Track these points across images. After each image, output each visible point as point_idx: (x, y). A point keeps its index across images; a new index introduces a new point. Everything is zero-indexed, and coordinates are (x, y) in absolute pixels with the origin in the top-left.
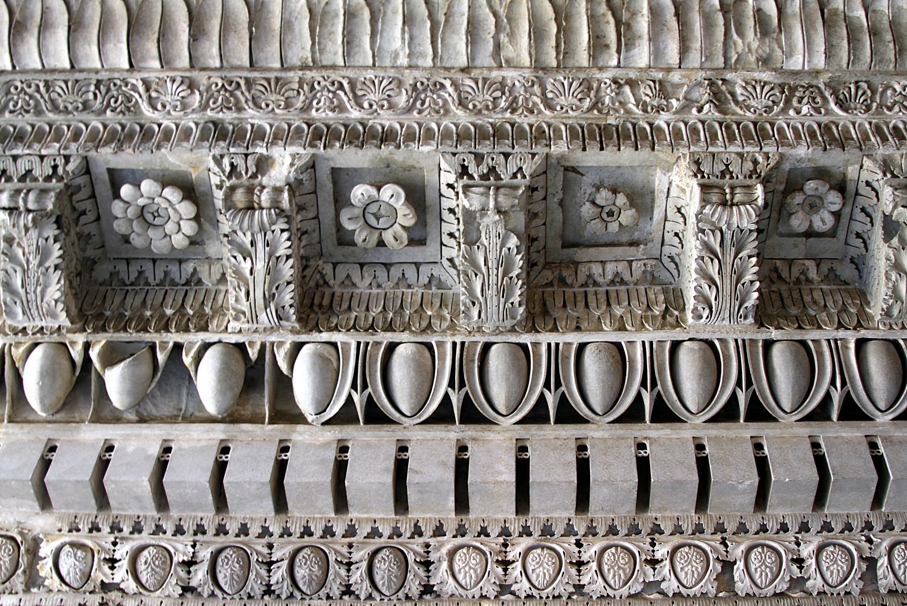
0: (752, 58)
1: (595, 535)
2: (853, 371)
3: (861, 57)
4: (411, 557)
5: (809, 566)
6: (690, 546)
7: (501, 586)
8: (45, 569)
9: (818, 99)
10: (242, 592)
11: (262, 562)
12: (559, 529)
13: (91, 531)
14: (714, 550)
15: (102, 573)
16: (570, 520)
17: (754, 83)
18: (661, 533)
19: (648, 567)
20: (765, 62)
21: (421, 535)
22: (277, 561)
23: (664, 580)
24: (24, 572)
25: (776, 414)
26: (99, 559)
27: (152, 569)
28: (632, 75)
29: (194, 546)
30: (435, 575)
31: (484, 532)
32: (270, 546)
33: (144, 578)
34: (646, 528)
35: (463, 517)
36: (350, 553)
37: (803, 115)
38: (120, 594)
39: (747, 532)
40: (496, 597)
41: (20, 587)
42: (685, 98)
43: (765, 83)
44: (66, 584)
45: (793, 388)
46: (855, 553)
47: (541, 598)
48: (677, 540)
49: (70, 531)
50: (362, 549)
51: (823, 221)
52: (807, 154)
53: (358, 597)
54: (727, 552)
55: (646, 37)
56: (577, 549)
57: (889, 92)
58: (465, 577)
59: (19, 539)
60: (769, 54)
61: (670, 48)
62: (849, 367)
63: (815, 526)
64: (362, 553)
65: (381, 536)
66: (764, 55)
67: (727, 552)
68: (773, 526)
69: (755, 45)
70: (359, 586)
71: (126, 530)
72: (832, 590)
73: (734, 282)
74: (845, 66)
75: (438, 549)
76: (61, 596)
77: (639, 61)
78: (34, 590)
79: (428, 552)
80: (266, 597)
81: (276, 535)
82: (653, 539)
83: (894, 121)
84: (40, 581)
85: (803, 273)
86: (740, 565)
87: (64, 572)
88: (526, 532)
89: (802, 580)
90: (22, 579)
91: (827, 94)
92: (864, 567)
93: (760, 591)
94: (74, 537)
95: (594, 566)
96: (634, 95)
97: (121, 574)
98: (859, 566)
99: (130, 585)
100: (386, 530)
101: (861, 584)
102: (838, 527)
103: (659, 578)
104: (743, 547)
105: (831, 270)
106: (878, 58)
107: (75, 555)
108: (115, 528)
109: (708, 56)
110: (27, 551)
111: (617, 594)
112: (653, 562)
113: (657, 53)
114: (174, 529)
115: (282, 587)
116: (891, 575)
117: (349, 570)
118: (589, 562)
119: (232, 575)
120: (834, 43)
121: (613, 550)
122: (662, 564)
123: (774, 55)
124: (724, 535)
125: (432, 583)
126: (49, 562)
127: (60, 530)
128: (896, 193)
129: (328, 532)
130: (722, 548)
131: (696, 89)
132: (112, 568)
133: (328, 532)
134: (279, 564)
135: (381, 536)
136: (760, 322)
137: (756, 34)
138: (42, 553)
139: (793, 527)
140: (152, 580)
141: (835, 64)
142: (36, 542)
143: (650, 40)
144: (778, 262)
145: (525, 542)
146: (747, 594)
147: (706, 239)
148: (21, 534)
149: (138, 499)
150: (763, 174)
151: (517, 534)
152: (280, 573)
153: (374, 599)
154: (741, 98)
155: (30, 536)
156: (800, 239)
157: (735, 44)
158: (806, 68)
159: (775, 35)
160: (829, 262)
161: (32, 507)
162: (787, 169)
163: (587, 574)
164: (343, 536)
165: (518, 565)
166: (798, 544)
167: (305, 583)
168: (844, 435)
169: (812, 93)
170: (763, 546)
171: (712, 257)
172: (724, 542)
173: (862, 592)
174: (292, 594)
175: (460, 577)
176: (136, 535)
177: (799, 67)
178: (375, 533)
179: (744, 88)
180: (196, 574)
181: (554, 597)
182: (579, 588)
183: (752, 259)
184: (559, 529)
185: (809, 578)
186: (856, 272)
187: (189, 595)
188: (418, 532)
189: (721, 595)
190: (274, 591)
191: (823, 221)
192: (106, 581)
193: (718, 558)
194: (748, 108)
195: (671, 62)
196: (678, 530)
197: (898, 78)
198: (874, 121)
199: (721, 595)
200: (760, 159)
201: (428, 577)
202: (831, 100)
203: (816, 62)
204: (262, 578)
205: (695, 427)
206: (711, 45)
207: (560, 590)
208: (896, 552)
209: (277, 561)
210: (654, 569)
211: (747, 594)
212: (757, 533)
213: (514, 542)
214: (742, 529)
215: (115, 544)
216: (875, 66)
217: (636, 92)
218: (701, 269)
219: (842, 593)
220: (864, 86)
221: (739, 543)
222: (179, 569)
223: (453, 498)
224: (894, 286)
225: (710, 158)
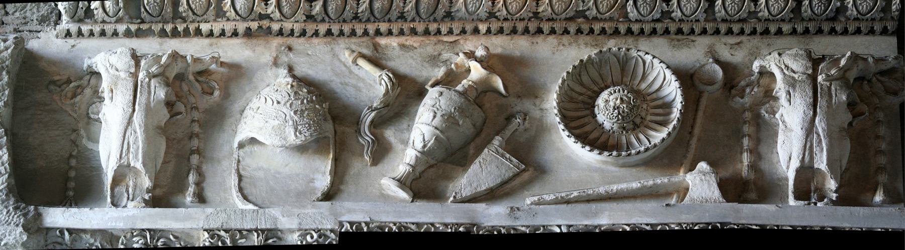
5: (673, 4)
7: (489, 13)
53: (406, 20)
76: (234, 23)
87: (238, 8)
90: (213, 13)
101: (705, 15)
116: (723, 11)
173: (706, 20)
207: (525, 16)
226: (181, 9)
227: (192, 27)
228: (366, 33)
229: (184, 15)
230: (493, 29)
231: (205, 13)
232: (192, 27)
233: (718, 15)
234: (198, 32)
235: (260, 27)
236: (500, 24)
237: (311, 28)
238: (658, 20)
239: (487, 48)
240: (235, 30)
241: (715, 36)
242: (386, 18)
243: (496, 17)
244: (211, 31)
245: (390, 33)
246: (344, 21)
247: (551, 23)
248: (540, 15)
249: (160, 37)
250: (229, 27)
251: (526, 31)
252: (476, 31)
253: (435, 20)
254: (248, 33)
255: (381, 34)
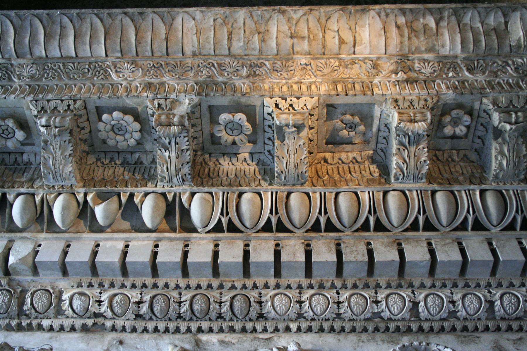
1: (346, 288)
4: (252, 299)
5: (458, 305)
6: (395, 294)
7: (298, 314)
8: (65, 305)
10: (166, 317)
11: (176, 302)
12: (328, 285)
13: (88, 287)
14: (408, 296)
15: (94, 308)
16: (333, 281)
18: (381, 287)
19: (374, 305)
20: (430, 50)
21: (257, 288)
22: (184, 302)
23: (382, 311)
24: (54, 307)
26: (93, 301)
27: (120, 306)
29: (141, 294)
30: (265, 308)
31: (289, 287)
32: (180, 294)
33: (116, 310)
34: (372, 284)
35: (279, 279)
36: (221, 297)
38: (103, 318)
39: (425, 287)
40: (296, 319)
41: (52, 315)
44: (76, 314)
46: (482, 298)
47: (319, 320)
48: (388, 291)
49: (78, 287)
50: (227, 295)
53: (225, 320)
54: (415, 297)
56: (337, 296)
58: (280, 309)
59: (52, 291)
63: (461, 284)
64: (227, 297)
65: (236, 288)
67: (415, 297)
68: (438, 284)
70: (226, 314)
71: (106, 286)
72: (471, 317)
73: (416, 161)
74: (471, 52)
75: (266, 295)
76: (73, 320)
78: (60, 317)
79: (261, 297)
80: (178, 320)
81: (183, 288)
82: (376, 291)
84: (62, 312)
85: (450, 157)
86: (422, 304)
87: (75, 307)
88: (311, 287)
89: (455, 312)
90: (53, 311)
91: (462, 66)
92: (488, 305)
93: (433, 318)
94: (80, 290)
95: (346, 304)
97: (104, 308)
98: (485, 305)
99: (109, 314)
100: (239, 285)
102: (473, 286)
103: (380, 310)
104: (423, 295)
105: (465, 155)
107: (81, 299)
108: (101, 285)
110: (56, 297)
111: (359, 318)
112: (377, 302)
114: (131, 285)
115: (187, 314)
116: (502, 310)
117: (220, 306)
118: (343, 302)
119: (161, 308)
121: (356, 296)
122: (381, 303)
124: (413, 289)
125: (263, 312)
126: (67, 302)
127: (73, 287)
129: (210, 287)
130: (412, 295)
132: (100, 305)
133: (210, 287)
134: (185, 303)
135: (236, 288)
138: (64, 298)
139: (449, 284)
140: (120, 311)
142: (61, 293)
145: (312, 292)
146: (426, 319)
148: (53, 288)
149: (113, 270)
151: (306, 288)
152: (185, 308)
153: (233, 321)
155: (57, 290)
160: (464, 151)
161: (58, 275)
163: (343, 308)
164: (218, 289)
165: (307, 303)
166: (452, 294)
167: (198, 312)
170: (433, 294)
171: (404, 148)
172: (413, 292)
174: (191, 318)
175: (278, 309)
176: (112, 289)
177: (447, 53)
178: (233, 287)
179: (419, 64)
180: (142, 308)
181: (326, 320)
182: (339, 315)
184: (328, 285)
185: (458, 311)
186: (478, 156)
187: (138, 319)
188: (255, 286)
189: (412, 319)
190: (182, 317)
191: (461, 130)
192: (96, 312)
193: (410, 301)
196: (389, 286)
198: (487, 79)
199: (412, 319)
201: (261, 309)
202: (465, 69)
204: (176, 310)
207: (329, 316)
208: (504, 298)
209: (184, 302)
210: (377, 306)
211: (426, 319)
212: (430, 288)
213: (304, 291)
214: (422, 286)
215: (101, 293)
219: (476, 319)
221: (421, 293)
222: (134, 306)
223: (273, 270)
226: (25, 308)
227: (35, 323)
228: (189, 330)
229: (27, 312)
230: (302, 328)
231: (46, 311)
232: (35, 323)
233: (498, 314)
234: (40, 327)
235: (95, 324)
236: (308, 323)
237: (140, 325)
238: (444, 320)
239: (298, 344)
240: (73, 326)
241: (496, 333)
242: (207, 318)
243: (305, 318)
244: (51, 326)
245: (211, 330)
246: (170, 320)
247: (352, 323)
248: (342, 316)
249: (7, 330)
250: (67, 323)
251: (332, 330)
252: (288, 329)
253: (251, 320)
254: (85, 329)
255: (203, 332)
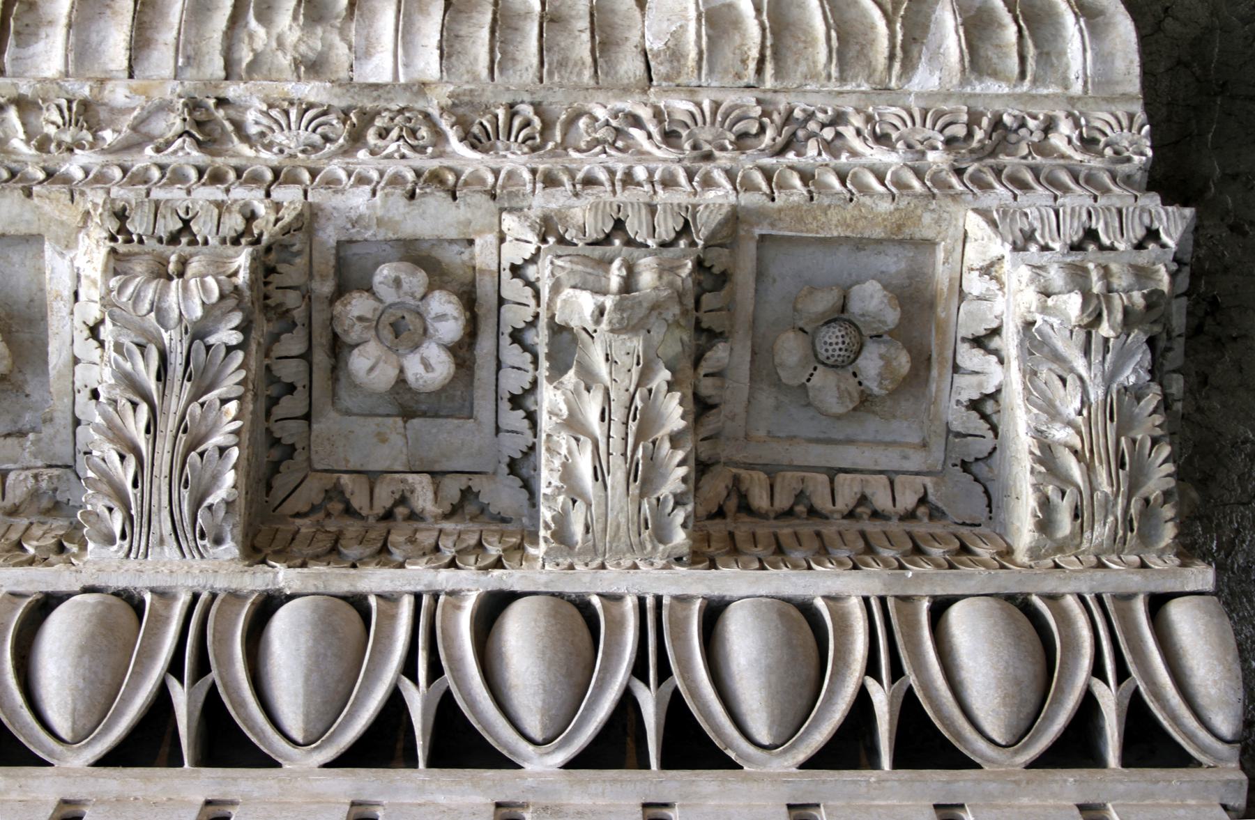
0: (285, 61)
2: (460, 647)
3: (519, 56)
9: (423, 132)
17: (286, 104)
20: (313, 67)
25: (270, 746)
28: (25, 88)
37: (389, 157)
42: (134, 128)
43: (310, 106)
45: (307, 679)
51: (429, 367)
52: (372, 207)
55: (63, 21)
57: (582, 123)
60: (321, 54)
61: (111, 41)
62: (451, 640)
66: (312, 55)
69: (292, 37)
73: (180, 448)
74: (484, 73)
77: (44, 66)
83: (586, 167)
85: (403, 500)
91: (444, 124)
96: (24, 124)
105: (467, 493)
106: (555, 58)
109: (189, 56)
113: (82, 51)
120: (462, 33)
123: (333, 54)
128: (558, 262)
131: (162, 116)
136: (255, 552)
137: (295, 18)
141: (463, 69)
143: (69, 26)
144: (345, 479)
147: (128, 366)
150: (265, 237)
154: (253, 130)
156: (390, 421)
157: (251, 36)
158: (402, 80)
159: (338, 23)
160: (464, 478)
162: (332, 242)
168: (441, 799)
169: (409, 120)
171: (137, 399)
177: (386, 77)
179: (266, 114)
183: (227, 406)
186: (524, 494)
191: (427, 366)
194: (269, 147)
195: (112, 66)
197: (601, 96)
198: (541, 167)
200: (261, 209)
202: (452, 135)
203: (421, 65)
205: (67, 774)
206: (200, 36)
216: (550, 73)
217: (32, 119)
218: (111, 426)
220: (527, 110)
224: (564, 465)
225: (148, 209)
